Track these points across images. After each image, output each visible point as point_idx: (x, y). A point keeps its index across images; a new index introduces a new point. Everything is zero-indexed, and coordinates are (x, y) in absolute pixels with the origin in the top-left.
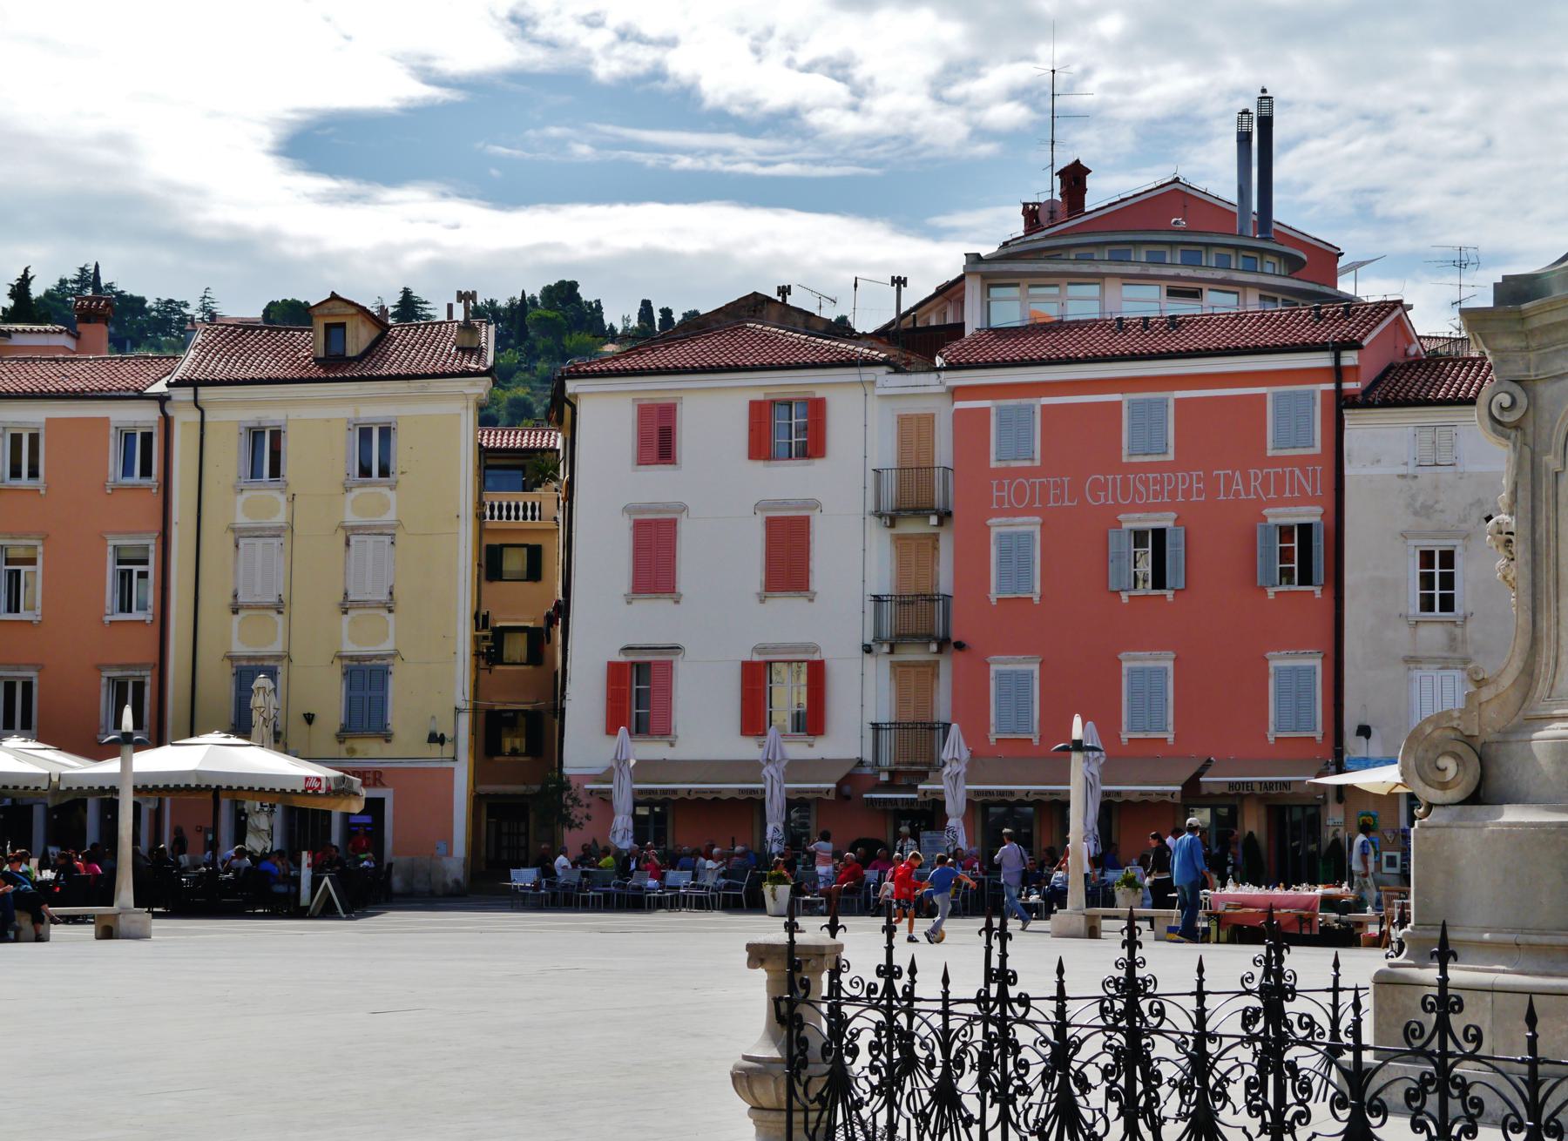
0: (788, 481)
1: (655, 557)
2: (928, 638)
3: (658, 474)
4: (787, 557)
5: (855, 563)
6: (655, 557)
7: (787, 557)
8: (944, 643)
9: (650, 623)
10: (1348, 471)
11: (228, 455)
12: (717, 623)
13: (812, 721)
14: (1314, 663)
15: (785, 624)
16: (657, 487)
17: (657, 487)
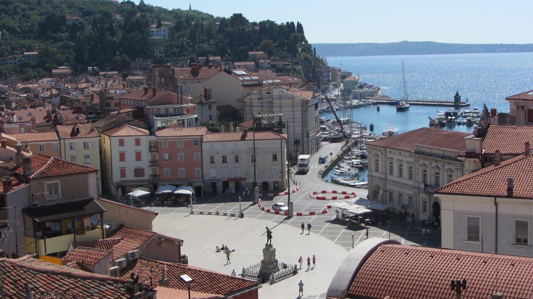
0: (138, 148)
1: (122, 157)
2: (156, 166)
3: (122, 147)
4: (138, 157)
5: (146, 157)
6: (122, 157)
7: (138, 157)
8: (158, 166)
9: (123, 164)
10: (203, 149)
11: (68, 147)
12: (131, 164)
13: (143, 175)
14: (200, 168)
15: (139, 165)
16: (122, 149)
17: (122, 149)
